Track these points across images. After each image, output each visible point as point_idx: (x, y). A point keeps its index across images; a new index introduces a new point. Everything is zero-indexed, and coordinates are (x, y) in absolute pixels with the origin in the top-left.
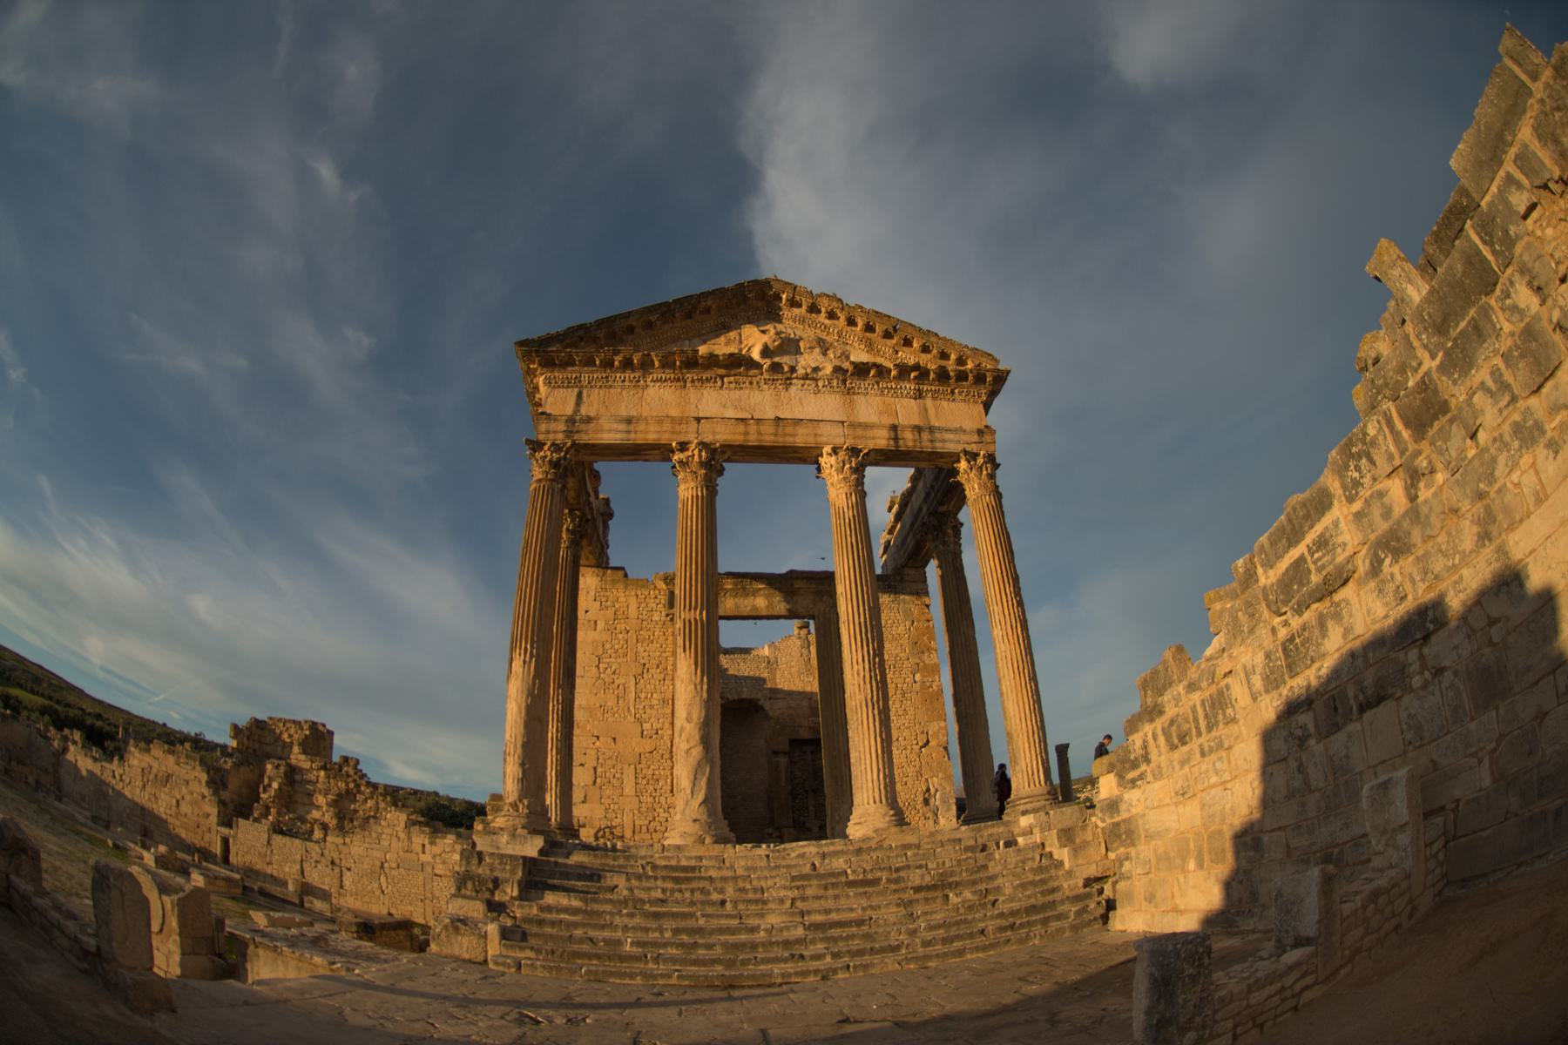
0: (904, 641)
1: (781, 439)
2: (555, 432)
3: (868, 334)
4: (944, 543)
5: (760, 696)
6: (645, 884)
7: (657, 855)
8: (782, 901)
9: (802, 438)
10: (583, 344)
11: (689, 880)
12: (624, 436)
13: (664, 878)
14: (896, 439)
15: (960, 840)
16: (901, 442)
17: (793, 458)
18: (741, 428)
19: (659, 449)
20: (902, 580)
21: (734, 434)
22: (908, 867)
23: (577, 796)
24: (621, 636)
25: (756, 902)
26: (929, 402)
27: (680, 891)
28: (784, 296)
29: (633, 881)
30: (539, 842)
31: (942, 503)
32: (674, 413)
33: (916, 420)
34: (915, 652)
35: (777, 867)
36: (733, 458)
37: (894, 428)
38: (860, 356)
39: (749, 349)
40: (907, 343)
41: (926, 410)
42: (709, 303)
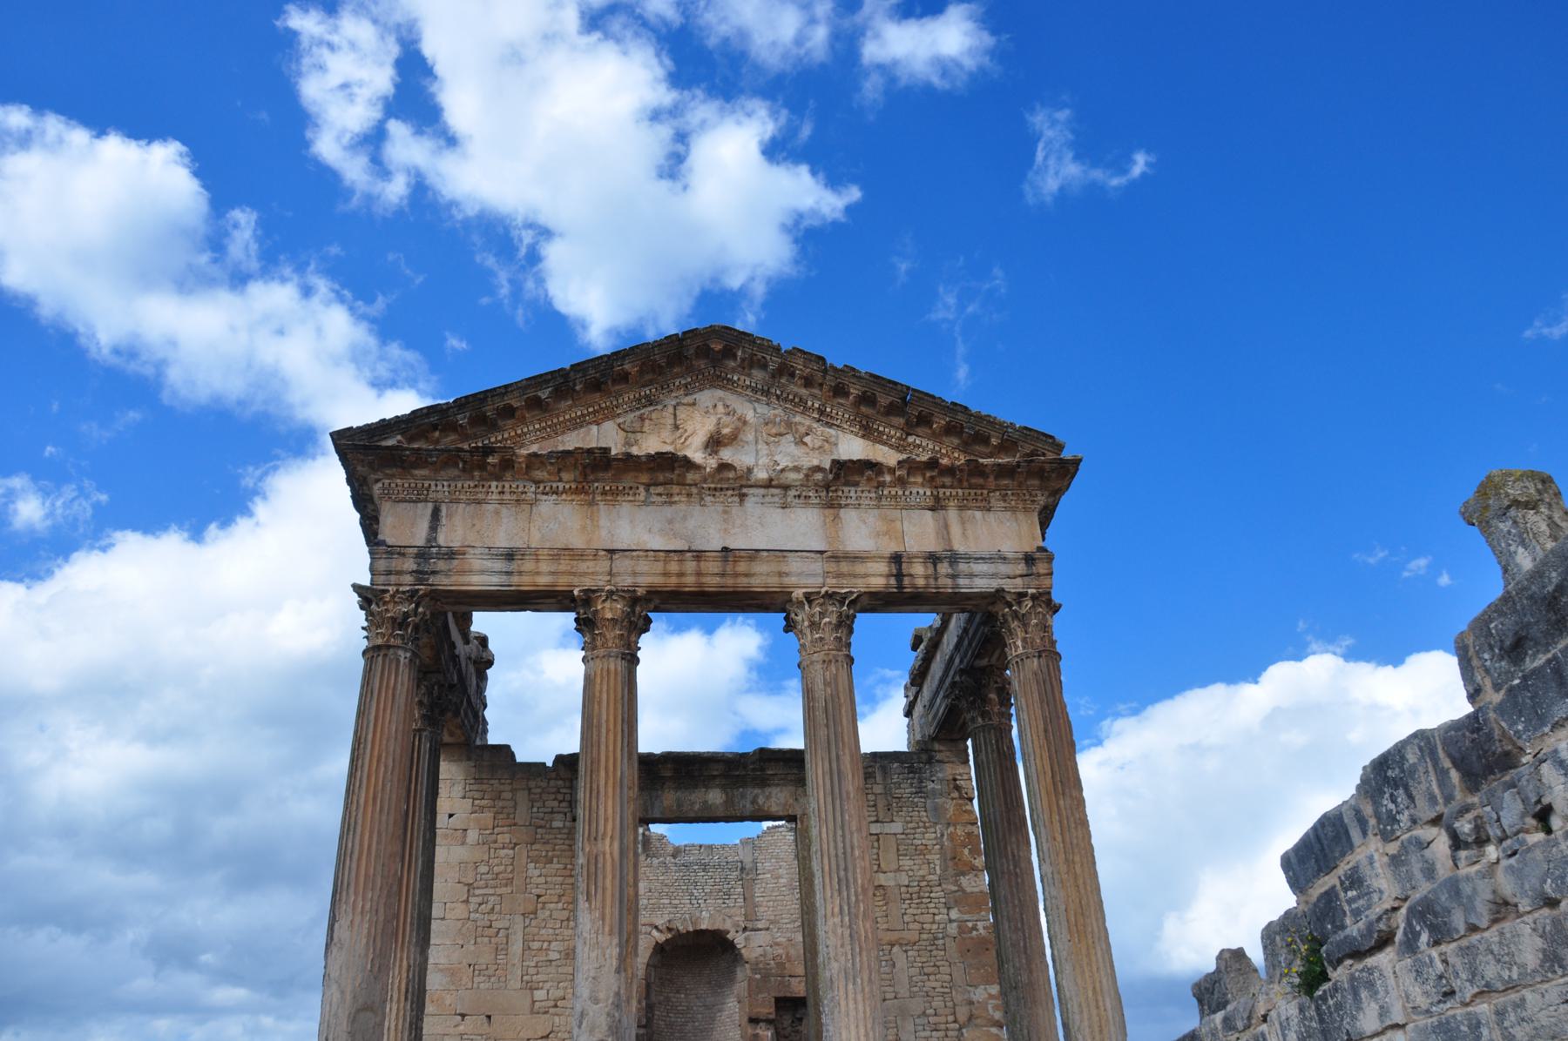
0: (935, 858)
1: (730, 581)
2: (399, 573)
3: (863, 409)
4: (984, 714)
5: (728, 925)
9: (761, 578)
10: (437, 434)
12: (503, 579)
14: (899, 576)
16: (906, 581)
18: (674, 567)
20: (930, 761)
21: (666, 574)
24: (503, 853)
26: (952, 514)
28: (739, 353)
31: (978, 656)
32: (578, 542)
33: (931, 544)
34: (951, 871)
36: (662, 606)
37: (897, 559)
38: (853, 447)
39: (686, 439)
40: (924, 420)
41: (946, 526)
42: (626, 367)
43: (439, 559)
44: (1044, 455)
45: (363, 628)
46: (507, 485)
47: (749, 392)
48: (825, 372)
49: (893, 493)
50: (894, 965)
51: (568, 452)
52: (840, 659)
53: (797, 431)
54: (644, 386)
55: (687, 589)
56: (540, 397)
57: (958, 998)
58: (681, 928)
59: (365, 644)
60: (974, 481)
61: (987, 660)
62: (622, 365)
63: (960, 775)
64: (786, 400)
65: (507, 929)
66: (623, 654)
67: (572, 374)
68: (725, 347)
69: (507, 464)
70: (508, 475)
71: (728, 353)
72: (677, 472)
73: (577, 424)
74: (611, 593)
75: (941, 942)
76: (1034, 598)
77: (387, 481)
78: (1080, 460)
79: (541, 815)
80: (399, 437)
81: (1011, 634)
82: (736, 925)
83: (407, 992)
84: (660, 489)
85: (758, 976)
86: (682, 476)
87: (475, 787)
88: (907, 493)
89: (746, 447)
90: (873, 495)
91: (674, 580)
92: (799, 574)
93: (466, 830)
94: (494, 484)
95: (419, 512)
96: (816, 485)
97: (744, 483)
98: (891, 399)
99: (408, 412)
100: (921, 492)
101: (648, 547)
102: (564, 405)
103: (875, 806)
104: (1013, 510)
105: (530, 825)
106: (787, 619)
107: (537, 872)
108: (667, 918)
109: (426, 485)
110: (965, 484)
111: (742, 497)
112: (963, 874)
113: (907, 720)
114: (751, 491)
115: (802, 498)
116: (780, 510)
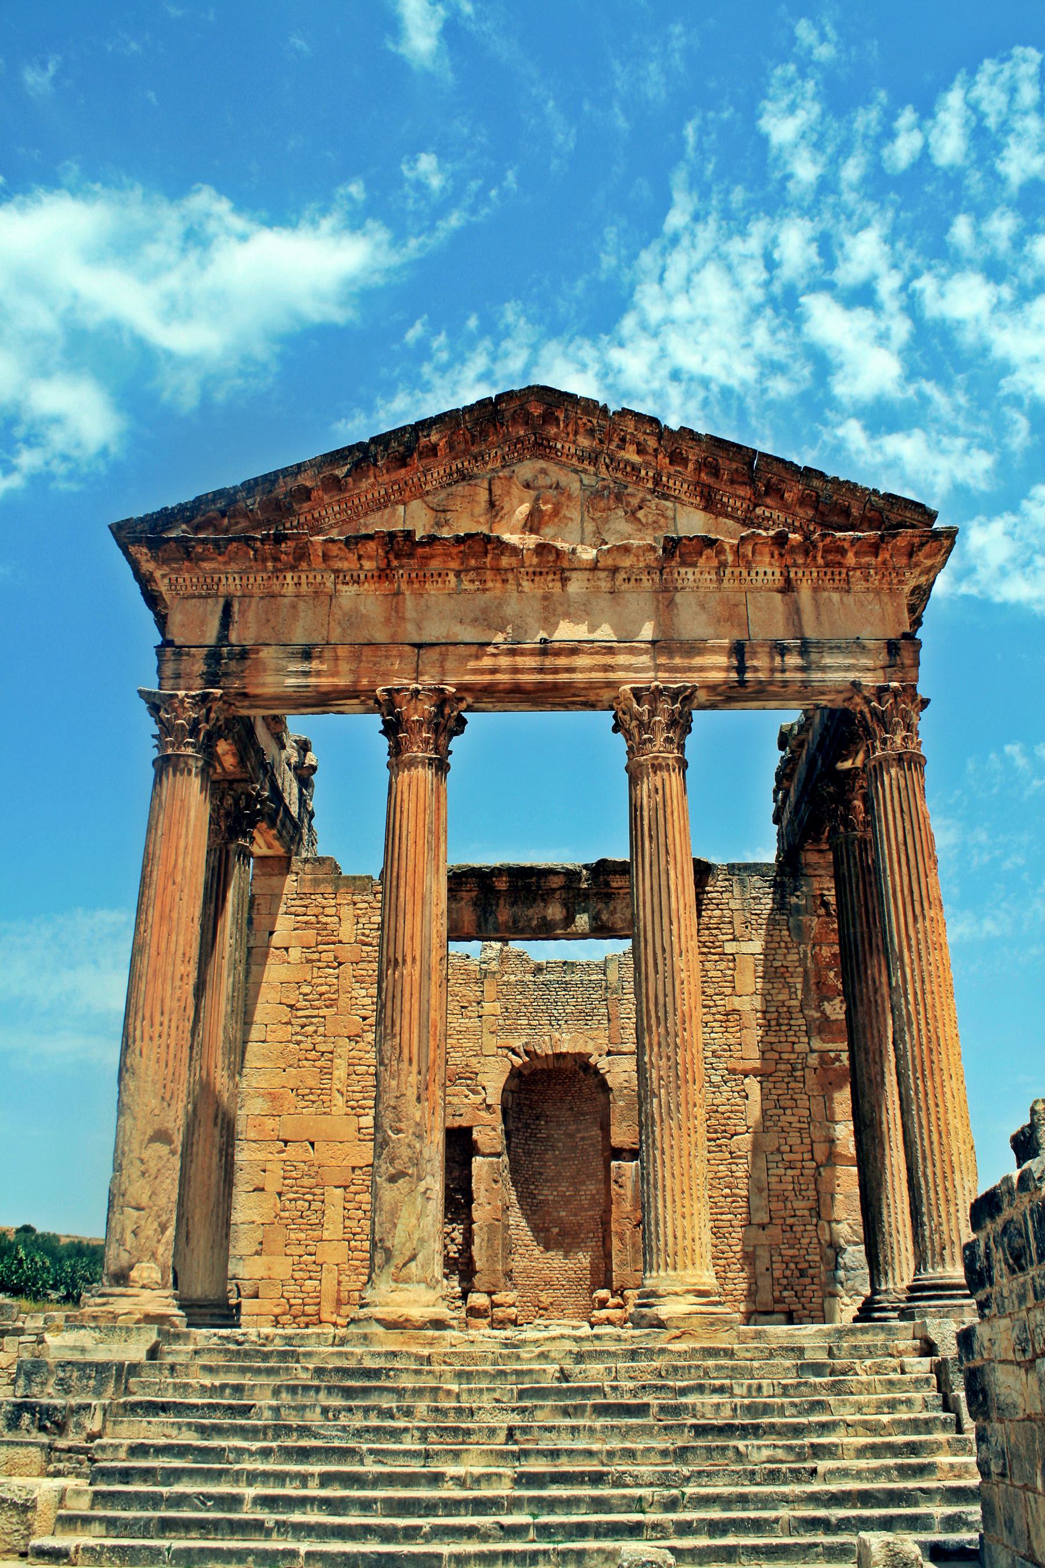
1: (549, 678)
3: (703, 475)
5: (590, 1048)
6: (301, 1400)
7: (331, 1349)
8: (492, 1431)
10: (226, 521)
11: (366, 1391)
13: (330, 1389)
14: (741, 669)
15: (801, 1350)
16: (748, 676)
17: (574, 703)
19: (357, 697)
22: (700, 1389)
23: (243, 1243)
25: (456, 1430)
27: (350, 1409)
28: (562, 417)
29: (284, 1395)
30: (151, 1335)
33: (779, 630)
34: (814, 995)
35: (502, 1373)
36: (476, 705)
40: (774, 490)
42: (434, 438)
43: (231, 659)
44: (913, 527)
45: (154, 736)
46: (304, 577)
47: (574, 461)
48: (660, 437)
49: (737, 573)
50: (747, 1097)
51: (369, 537)
52: (670, 762)
53: (628, 504)
54: (455, 459)
55: (501, 687)
56: (337, 477)
57: (817, 1134)
58: (539, 1051)
59: (155, 754)
60: (830, 557)
61: (850, 761)
62: (429, 435)
63: (829, 889)
64: (617, 469)
65: (331, 1053)
66: (430, 759)
67: (372, 448)
68: (546, 410)
69: (302, 555)
70: (304, 565)
71: (549, 418)
72: (490, 556)
73: (381, 504)
74: (417, 692)
75: (799, 1073)
76: (896, 693)
77: (174, 576)
78: (956, 532)
79: (367, 932)
80: (184, 527)
81: (869, 734)
82: (599, 1048)
83: (216, 1117)
84: (472, 575)
85: (621, 1103)
86: (497, 557)
87: (297, 903)
88: (753, 574)
89: (570, 524)
90: (714, 577)
91: (487, 678)
92: (627, 668)
93: (287, 949)
94: (289, 575)
95: (209, 608)
96: (648, 566)
97: (565, 564)
98: (734, 466)
99: (192, 499)
100: (769, 571)
101: (459, 639)
102: (364, 484)
103: (731, 922)
104: (878, 592)
105: (356, 942)
106: (615, 717)
107: (363, 992)
108: (525, 1040)
109: (216, 579)
110: (820, 561)
111: (564, 581)
112: (829, 1000)
113: (776, 827)
114: (574, 575)
115: (633, 581)
116: (608, 596)
